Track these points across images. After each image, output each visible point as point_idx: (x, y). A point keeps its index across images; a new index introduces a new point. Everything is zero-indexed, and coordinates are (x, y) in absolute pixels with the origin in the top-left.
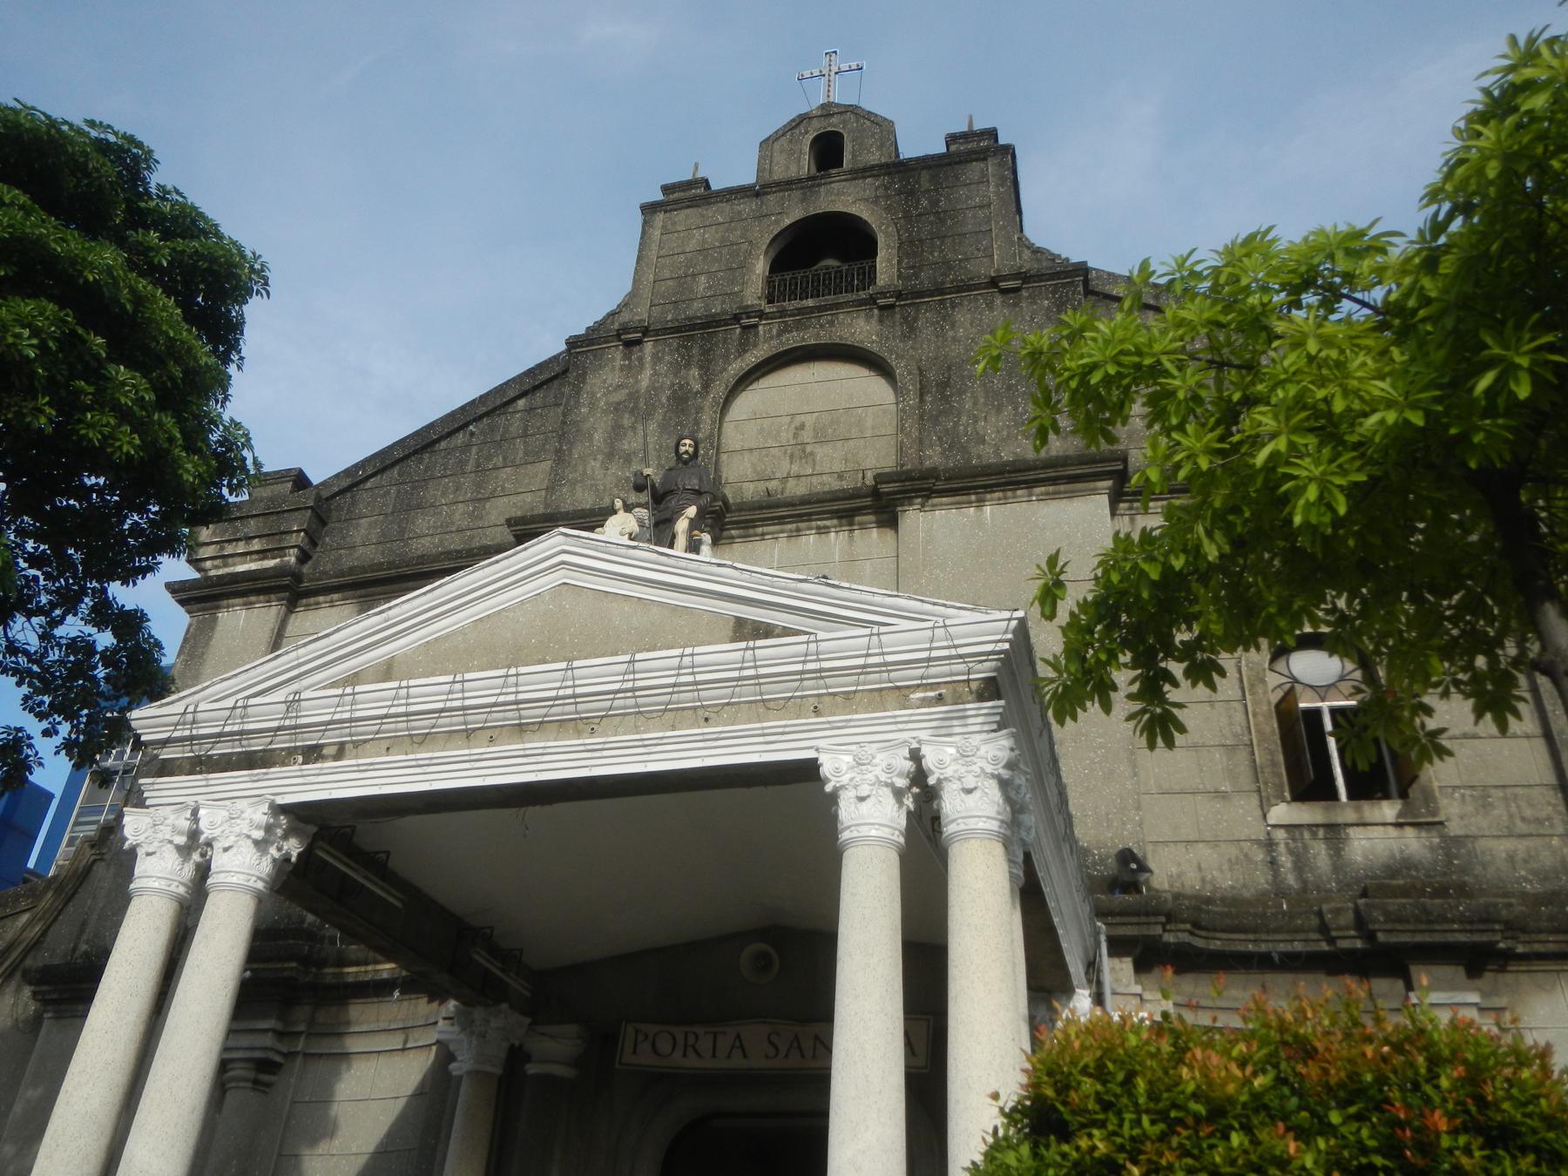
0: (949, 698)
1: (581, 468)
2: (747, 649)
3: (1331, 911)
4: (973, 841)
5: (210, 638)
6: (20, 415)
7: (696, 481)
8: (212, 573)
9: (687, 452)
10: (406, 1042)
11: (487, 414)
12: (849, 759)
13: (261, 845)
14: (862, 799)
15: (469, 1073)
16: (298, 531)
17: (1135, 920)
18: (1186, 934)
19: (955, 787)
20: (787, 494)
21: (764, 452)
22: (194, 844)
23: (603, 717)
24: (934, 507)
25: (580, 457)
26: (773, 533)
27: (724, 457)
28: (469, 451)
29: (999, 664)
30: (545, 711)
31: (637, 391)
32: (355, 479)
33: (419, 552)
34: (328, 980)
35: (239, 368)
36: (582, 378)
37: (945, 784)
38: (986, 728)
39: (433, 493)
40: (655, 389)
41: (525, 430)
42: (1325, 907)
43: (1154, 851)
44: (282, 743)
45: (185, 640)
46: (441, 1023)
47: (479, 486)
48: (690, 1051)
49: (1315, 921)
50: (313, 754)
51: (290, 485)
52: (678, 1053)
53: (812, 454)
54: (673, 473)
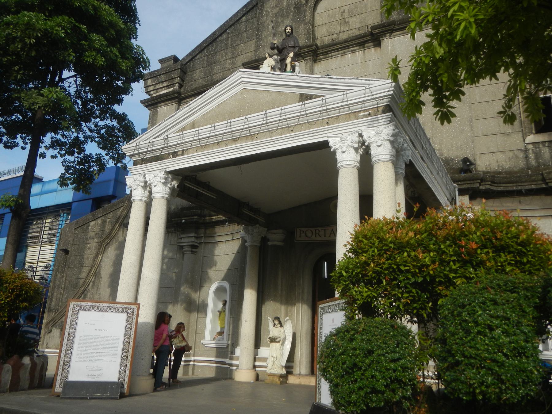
0: (373, 115)
1: (265, 40)
2: (302, 104)
3: (546, 173)
4: (381, 163)
5: (157, 117)
6: (64, 57)
7: (293, 43)
8: (154, 95)
9: (288, 32)
10: (233, 238)
11: (233, 25)
12: (339, 139)
13: (165, 184)
14: (343, 152)
16: (177, 77)
17: (469, 182)
18: (489, 186)
19: (374, 145)
20: (339, 39)
21: (330, 24)
22: (146, 185)
23: (257, 134)
25: (265, 36)
26: (335, 55)
27: (316, 28)
28: (228, 40)
29: (390, 99)
30: (239, 134)
31: (283, 7)
32: (193, 56)
33: (216, 79)
34: (207, 221)
35: (140, 25)
36: (263, 5)
37: (371, 144)
38: (385, 123)
39: (218, 57)
40: (289, 5)
41: (246, 29)
42: (544, 172)
43: (480, 157)
44: (165, 152)
45: (150, 119)
46: (241, 231)
47: (233, 52)
48: (317, 235)
49: (540, 177)
50: (175, 154)
51: (172, 61)
52: (314, 236)
53: (348, 22)
54: (285, 41)
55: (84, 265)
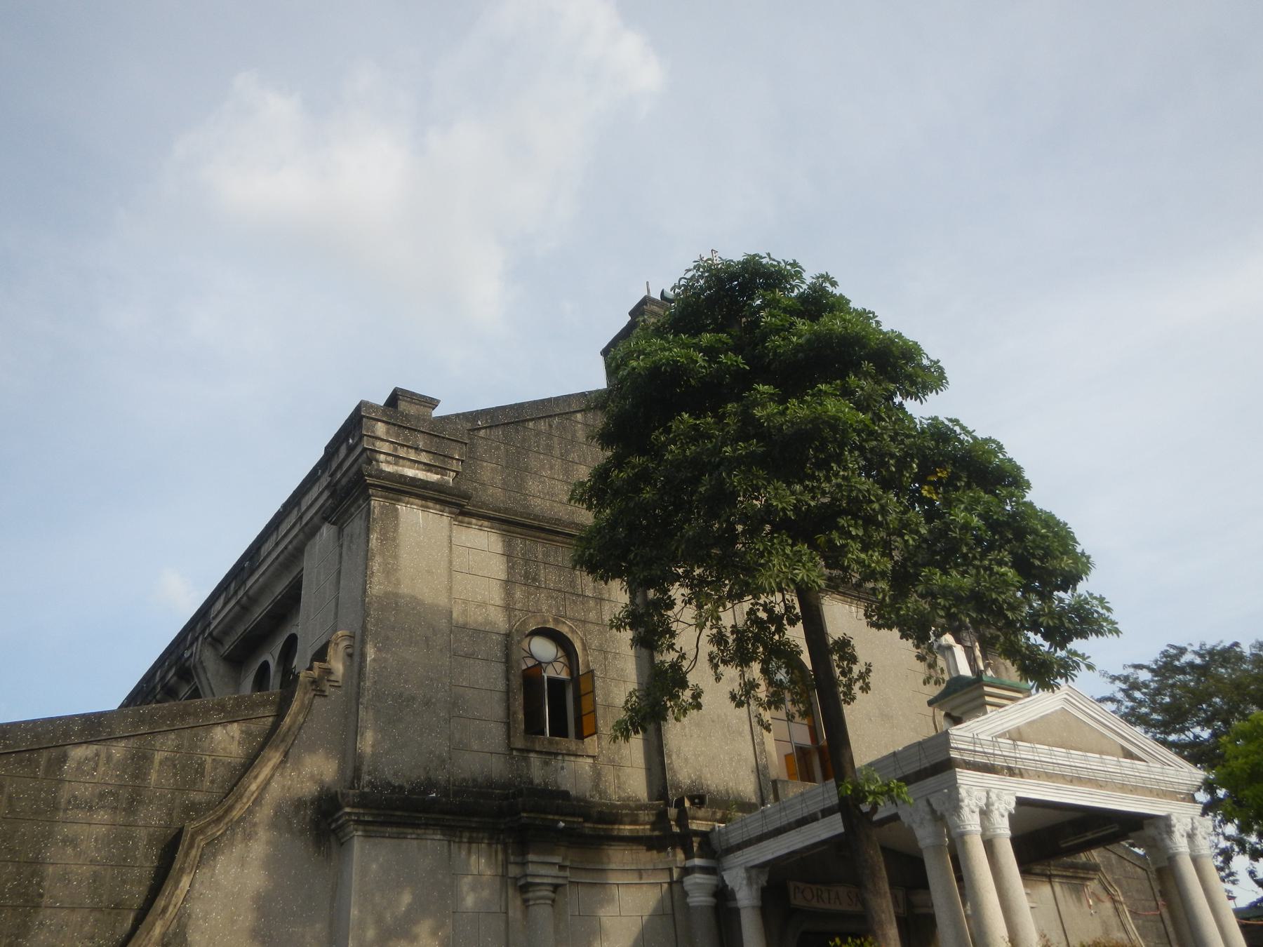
5: (397, 526)
10: (641, 878)
15: (753, 907)
50: (1011, 772)
55: (46, 900)
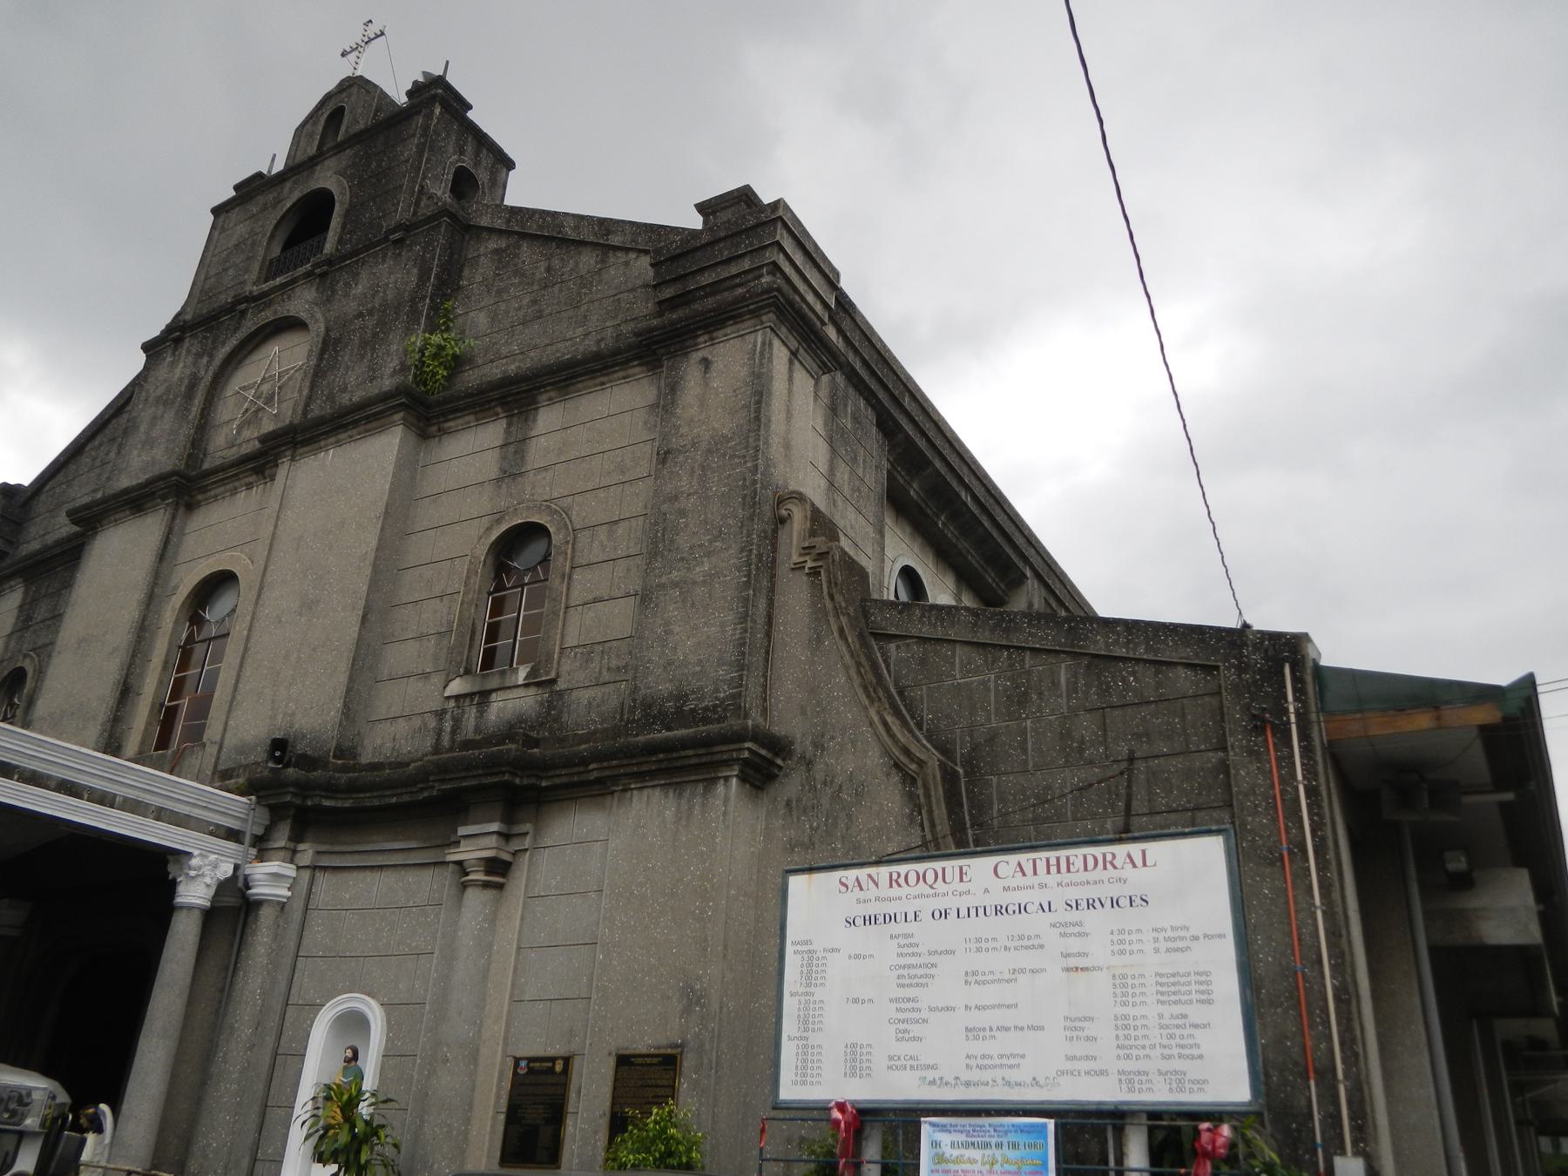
24: (303, 456)
